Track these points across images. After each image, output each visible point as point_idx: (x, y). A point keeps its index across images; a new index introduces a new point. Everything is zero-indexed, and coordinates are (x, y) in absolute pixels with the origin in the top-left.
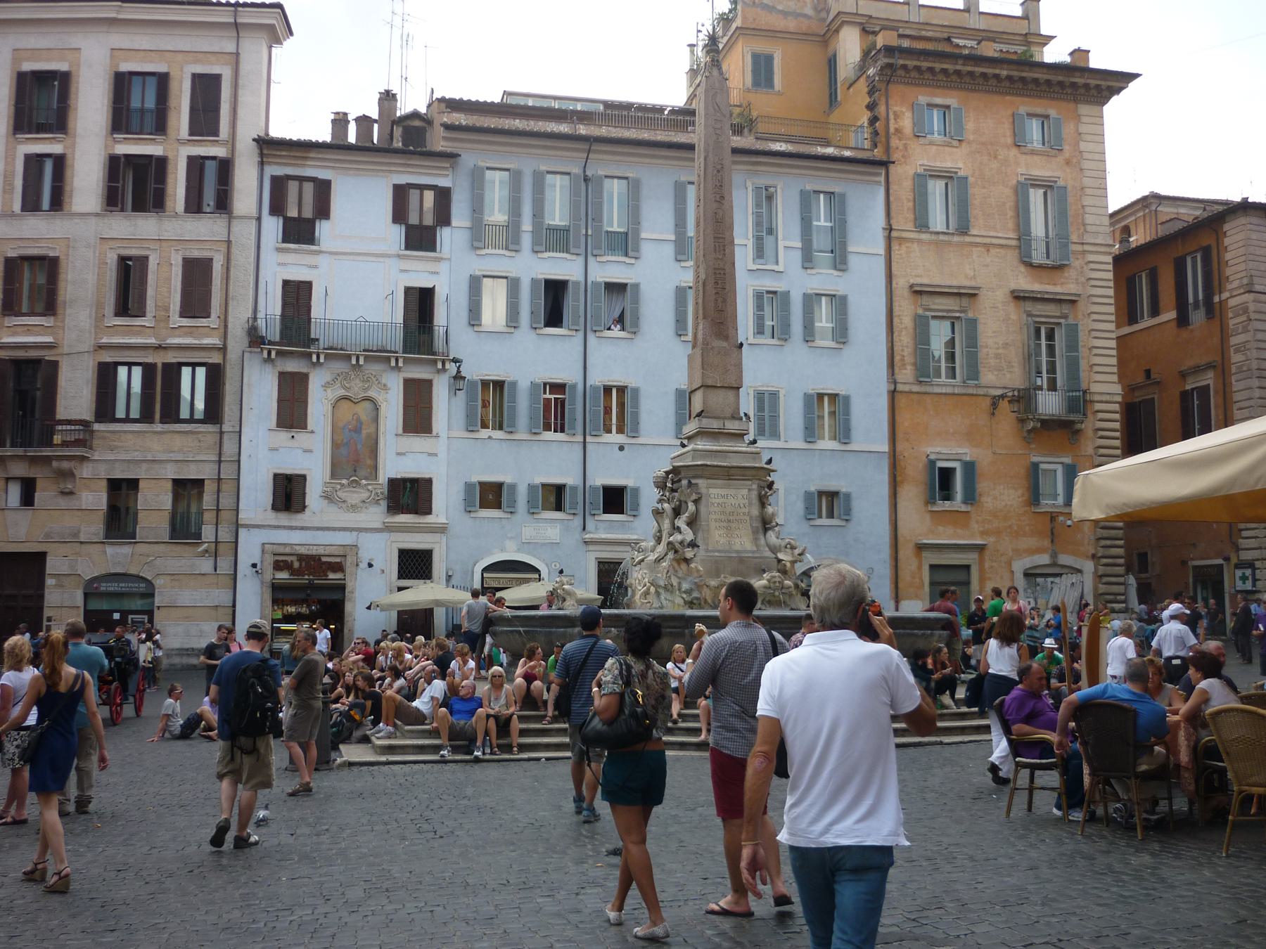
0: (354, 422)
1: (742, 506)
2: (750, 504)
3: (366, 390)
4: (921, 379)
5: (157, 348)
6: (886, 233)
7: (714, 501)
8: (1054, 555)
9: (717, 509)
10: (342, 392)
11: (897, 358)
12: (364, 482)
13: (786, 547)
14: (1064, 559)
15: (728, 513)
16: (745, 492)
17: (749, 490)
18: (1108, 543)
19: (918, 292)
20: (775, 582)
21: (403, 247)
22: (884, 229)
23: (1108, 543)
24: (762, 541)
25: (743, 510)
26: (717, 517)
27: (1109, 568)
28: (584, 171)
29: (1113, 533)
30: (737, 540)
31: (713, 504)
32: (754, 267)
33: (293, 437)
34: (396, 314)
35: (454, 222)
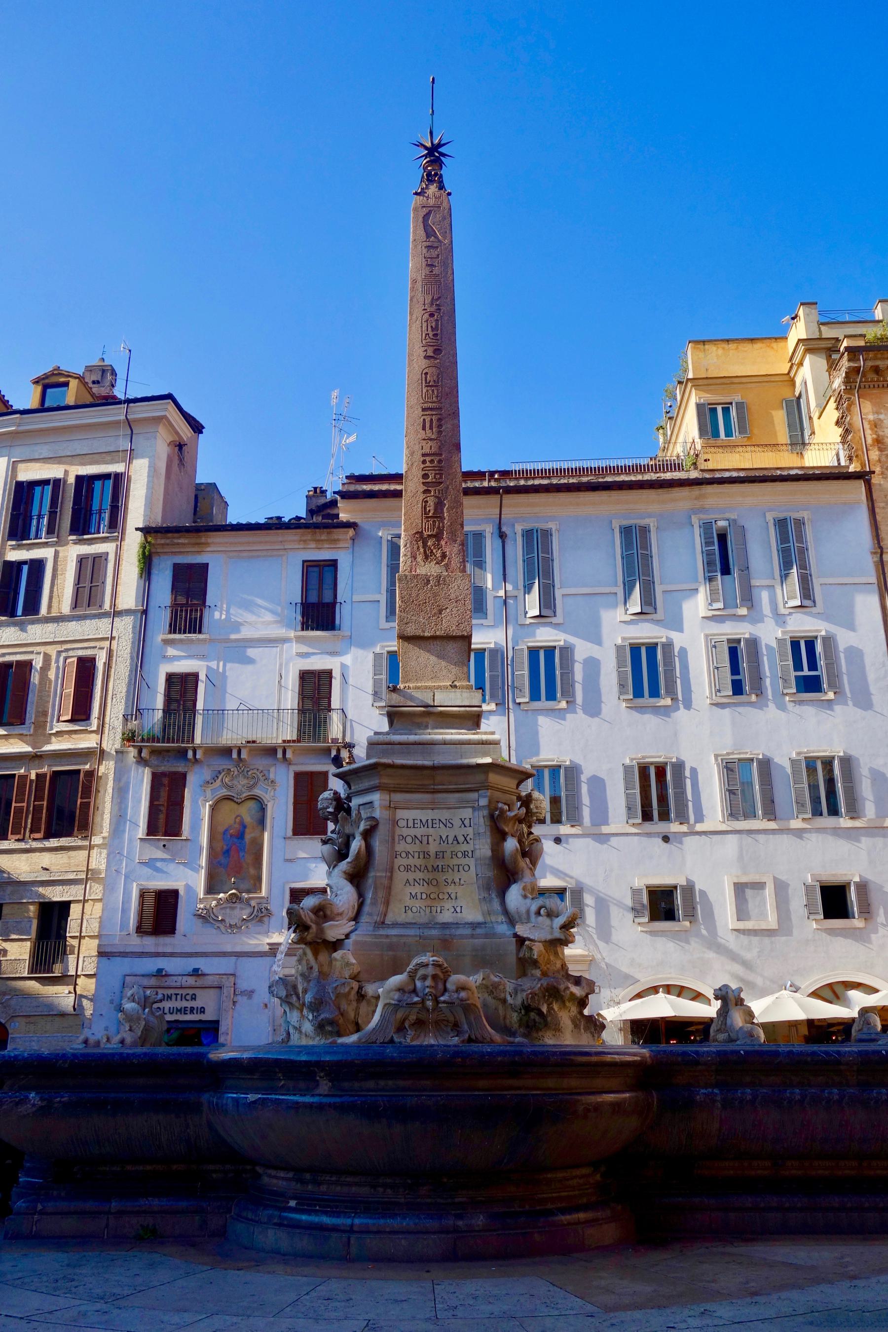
0: (237, 826)
3: (251, 787)
5: (33, 757)
6: (877, 558)
7: (405, 832)
9: (410, 848)
10: (224, 792)
12: (245, 895)
13: (538, 913)
15: (432, 854)
16: (467, 813)
20: (424, 978)
22: (872, 553)
25: (464, 847)
26: (410, 861)
28: (500, 528)
31: (404, 838)
32: (710, 613)
33: (164, 846)
34: (290, 699)
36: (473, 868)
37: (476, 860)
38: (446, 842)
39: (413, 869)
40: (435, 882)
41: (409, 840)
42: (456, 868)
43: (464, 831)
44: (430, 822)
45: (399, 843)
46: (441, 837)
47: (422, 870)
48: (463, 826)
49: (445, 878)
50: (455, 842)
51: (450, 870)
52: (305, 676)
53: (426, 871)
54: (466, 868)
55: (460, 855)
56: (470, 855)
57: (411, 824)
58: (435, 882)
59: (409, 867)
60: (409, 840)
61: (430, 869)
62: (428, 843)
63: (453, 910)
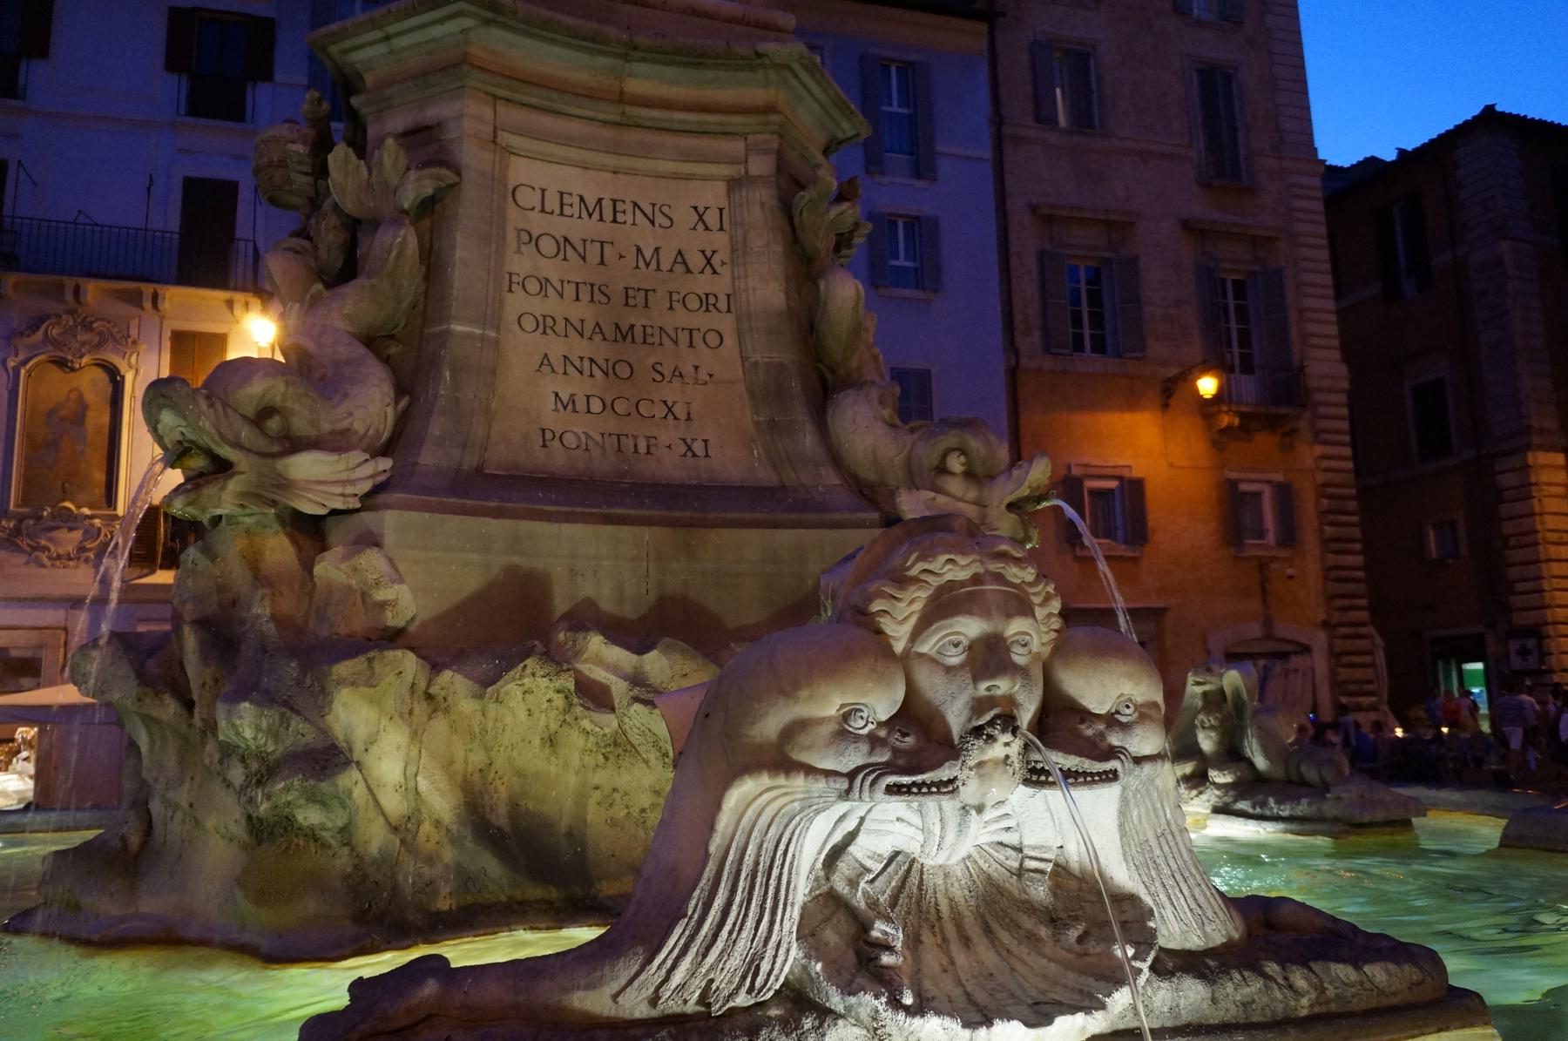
1: (696, 261)
2: (739, 251)
4: (1055, 351)
7: (537, 223)
8: (1268, 623)
9: (551, 269)
11: (1018, 318)
14: (1284, 629)
17: (733, 184)
18: (1346, 602)
19: (1047, 219)
21: (182, 111)
23: (1346, 602)
24: (808, 440)
25: (704, 283)
26: (551, 306)
27: (1349, 642)
29: (1352, 587)
30: (668, 434)
31: (535, 241)
35: (279, 77)
36: (730, 341)
37: (738, 319)
38: (653, 265)
39: (560, 327)
40: (624, 371)
41: (548, 246)
42: (683, 337)
43: (701, 240)
44: (607, 204)
45: (519, 251)
46: (639, 250)
47: (587, 333)
48: (700, 226)
49: (652, 360)
50: (680, 268)
51: (666, 341)
52: (192, 187)
53: (597, 338)
54: (713, 339)
55: (693, 303)
56: (722, 305)
57: (552, 203)
58: (624, 371)
59: (549, 322)
60: (548, 246)
61: (610, 333)
62: (602, 263)
63: (683, 449)
